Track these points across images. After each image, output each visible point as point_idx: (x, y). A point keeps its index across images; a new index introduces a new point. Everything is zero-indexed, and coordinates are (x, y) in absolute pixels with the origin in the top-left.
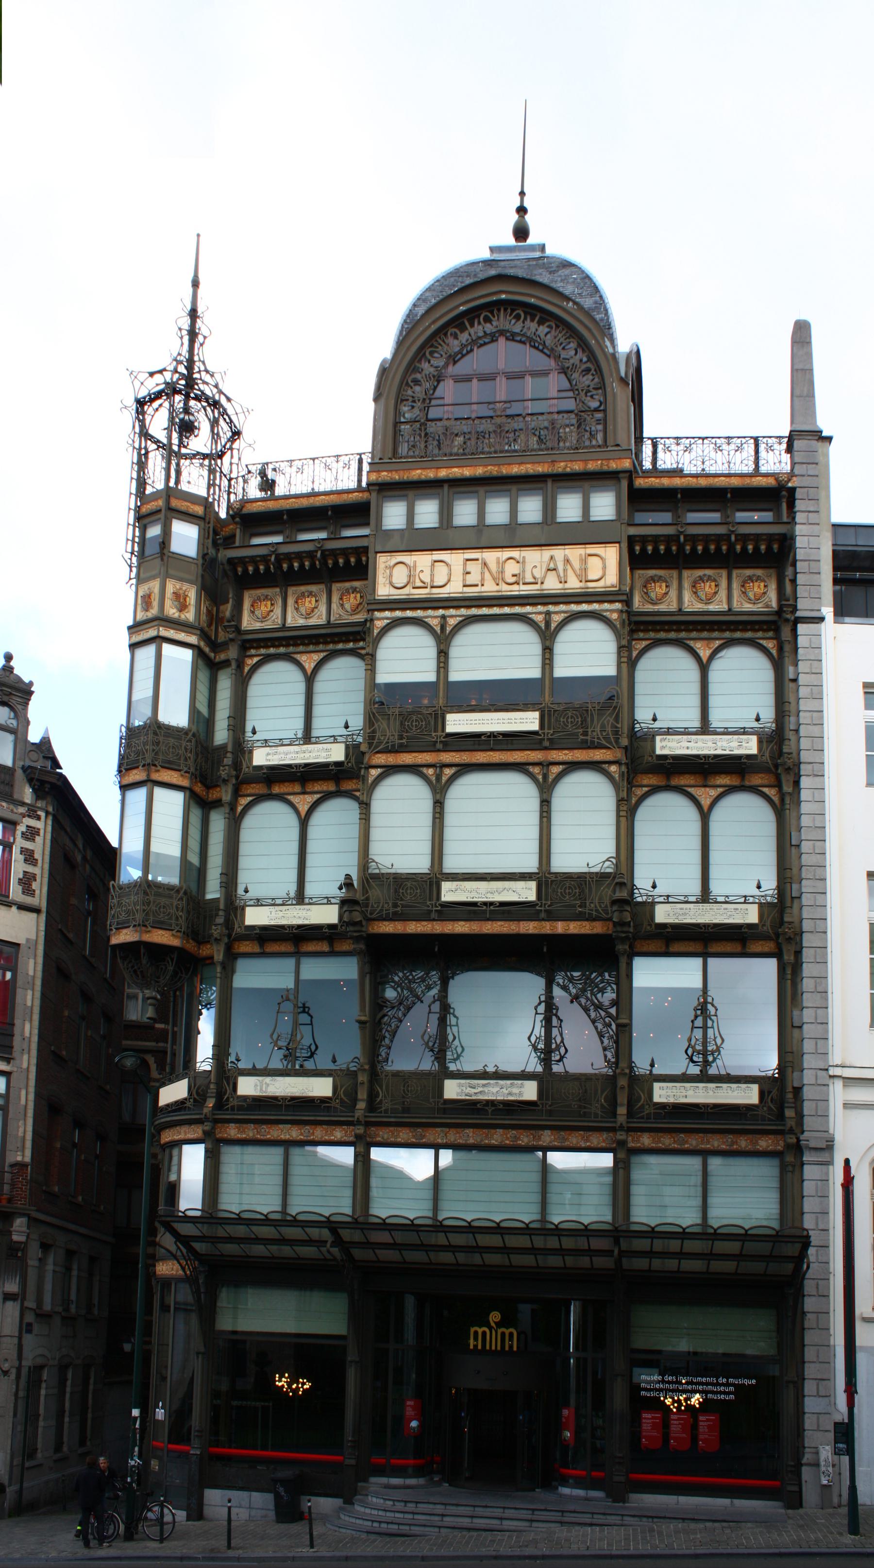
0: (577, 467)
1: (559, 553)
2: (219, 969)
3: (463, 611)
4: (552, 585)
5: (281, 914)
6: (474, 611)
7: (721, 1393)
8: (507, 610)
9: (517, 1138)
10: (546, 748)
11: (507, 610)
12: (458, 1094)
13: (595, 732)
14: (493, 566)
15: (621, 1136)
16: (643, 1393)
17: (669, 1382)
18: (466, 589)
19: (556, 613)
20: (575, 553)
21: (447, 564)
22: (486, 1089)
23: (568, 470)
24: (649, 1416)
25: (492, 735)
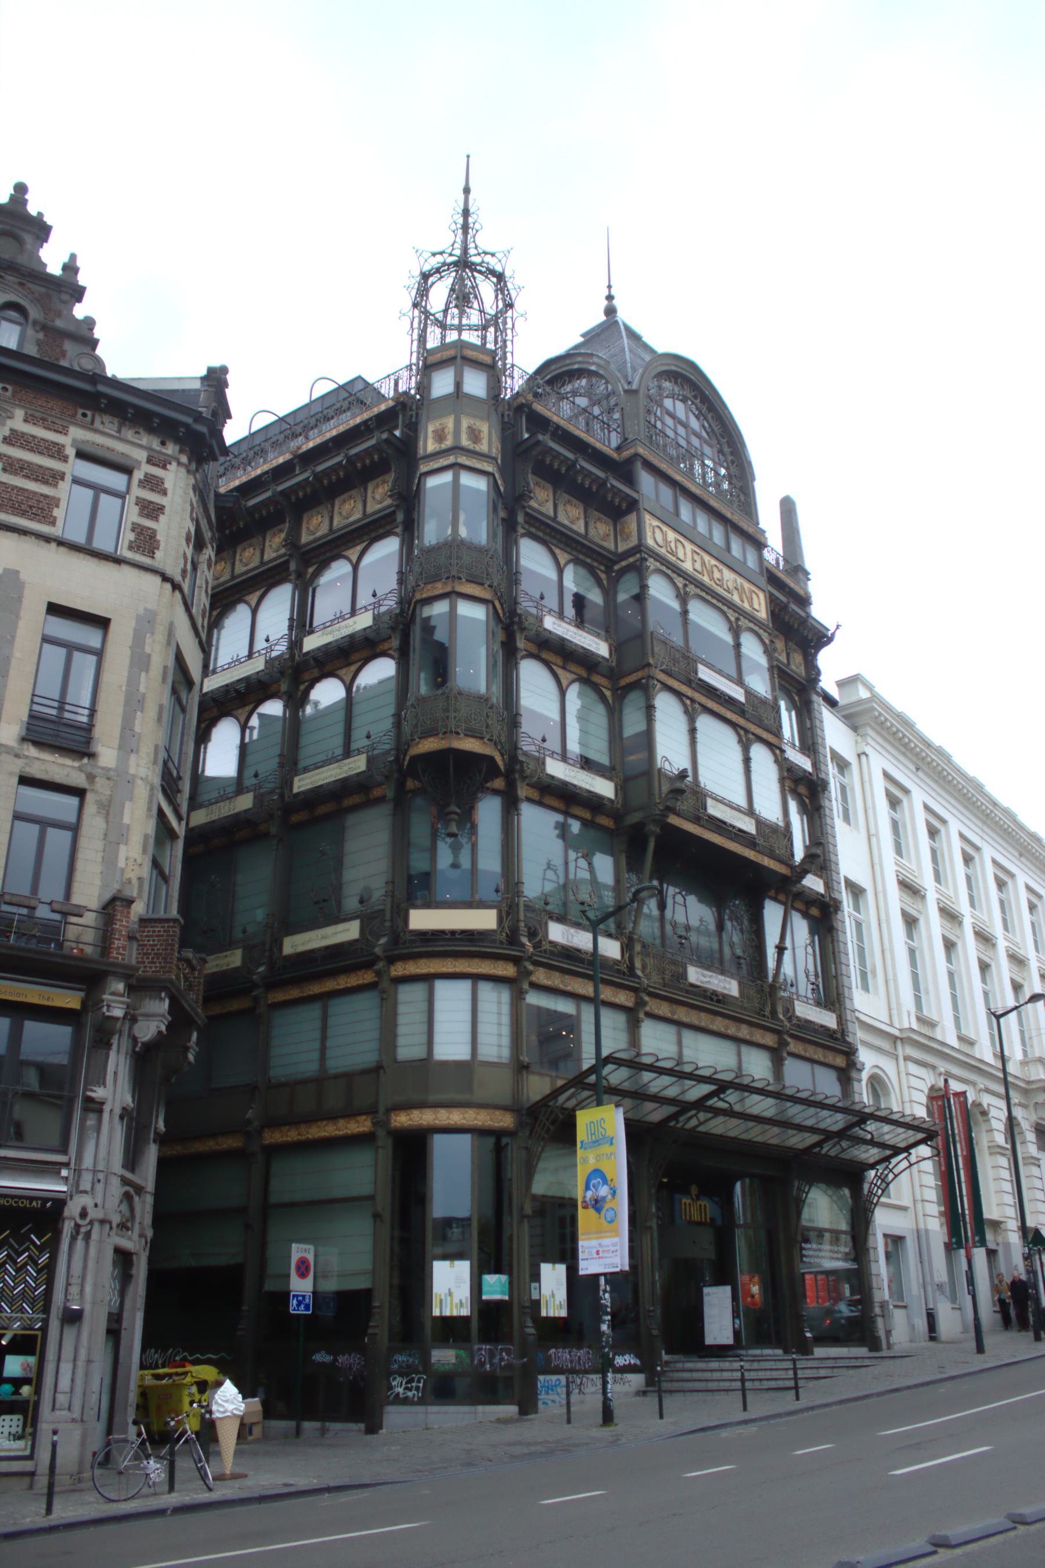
1: (740, 580)
4: (736, 598)
5: (573, 774)
8: (714, 601)
9: (727, 1028)
10: (747, 720)
11: (714, 601)
12: (697, 979)
20: (746, 585)
21: (684, 547)
22: (712, 980)
25: (722, 693)
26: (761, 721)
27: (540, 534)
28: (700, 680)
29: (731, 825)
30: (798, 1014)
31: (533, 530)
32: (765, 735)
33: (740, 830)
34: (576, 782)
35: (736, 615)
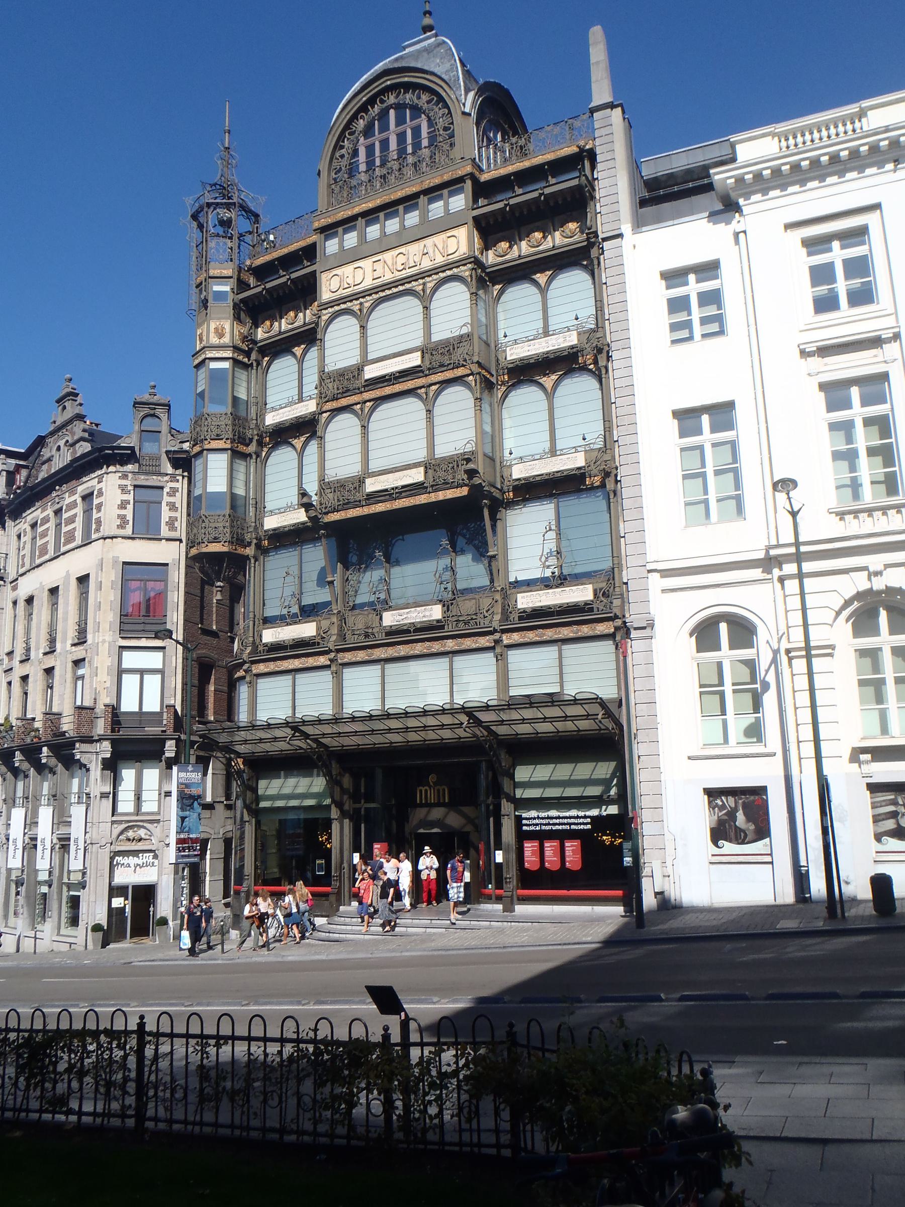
0: (437, 181)
2: (253, 561)
3: (375, 296)
4: (426, 264)
6: (382, 294)
7: (580, 824)
8: (401, 288)
11: (401, 288)
13: (457, 356)
14: (390, 263)
15: (497, 636)
16: (525, 828)
17: (542, 818)
18: (375, 281)
19: (430, 282)
20: (438, 239)
23: (432, 185)
24: (530, 845)
25: (392, 374)
26: (442, 366)
27: (284, 346)
28: (366, 381)
29: (393, 489)
30: (520, 606)
31: (278, 348)
32: (449, 375)
33: (403, 487)
34: (286, 523)
35: (421, 281)
